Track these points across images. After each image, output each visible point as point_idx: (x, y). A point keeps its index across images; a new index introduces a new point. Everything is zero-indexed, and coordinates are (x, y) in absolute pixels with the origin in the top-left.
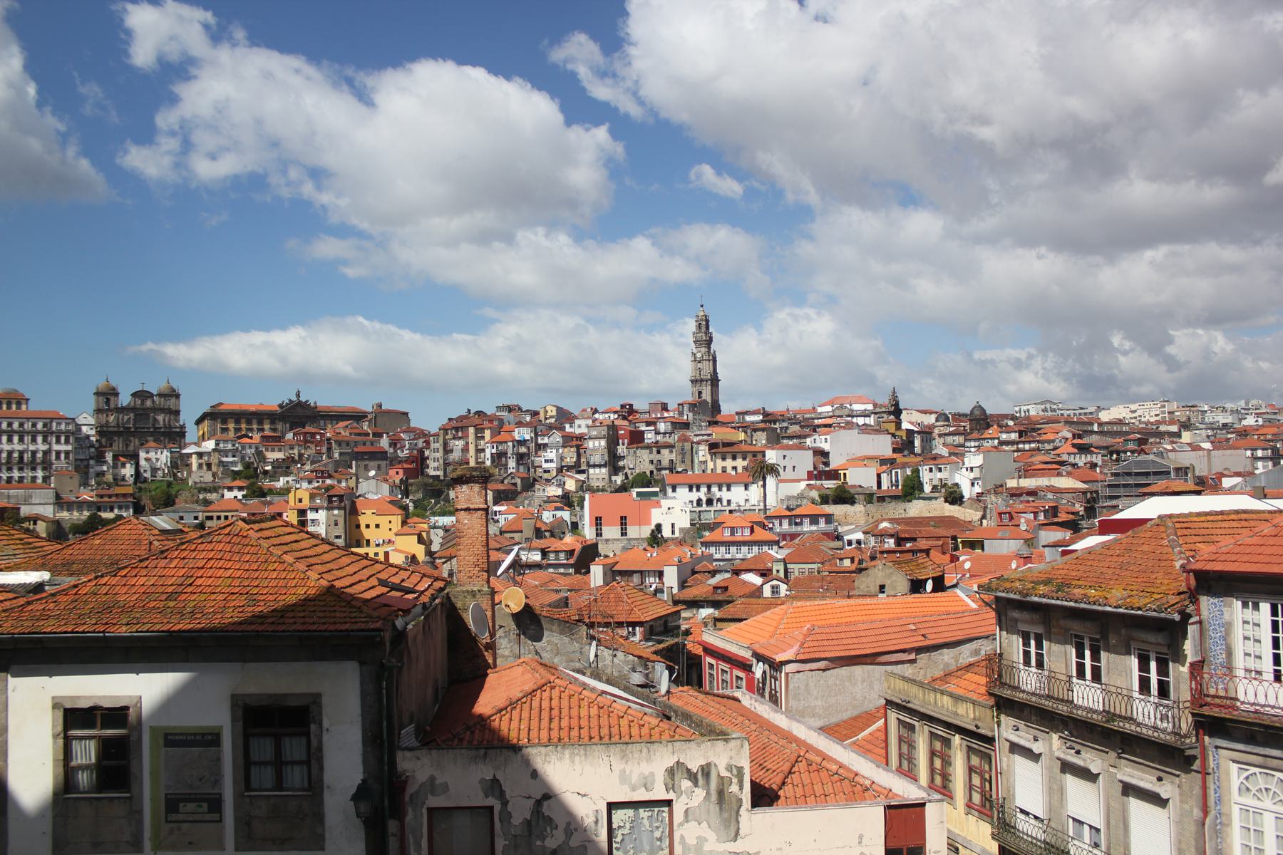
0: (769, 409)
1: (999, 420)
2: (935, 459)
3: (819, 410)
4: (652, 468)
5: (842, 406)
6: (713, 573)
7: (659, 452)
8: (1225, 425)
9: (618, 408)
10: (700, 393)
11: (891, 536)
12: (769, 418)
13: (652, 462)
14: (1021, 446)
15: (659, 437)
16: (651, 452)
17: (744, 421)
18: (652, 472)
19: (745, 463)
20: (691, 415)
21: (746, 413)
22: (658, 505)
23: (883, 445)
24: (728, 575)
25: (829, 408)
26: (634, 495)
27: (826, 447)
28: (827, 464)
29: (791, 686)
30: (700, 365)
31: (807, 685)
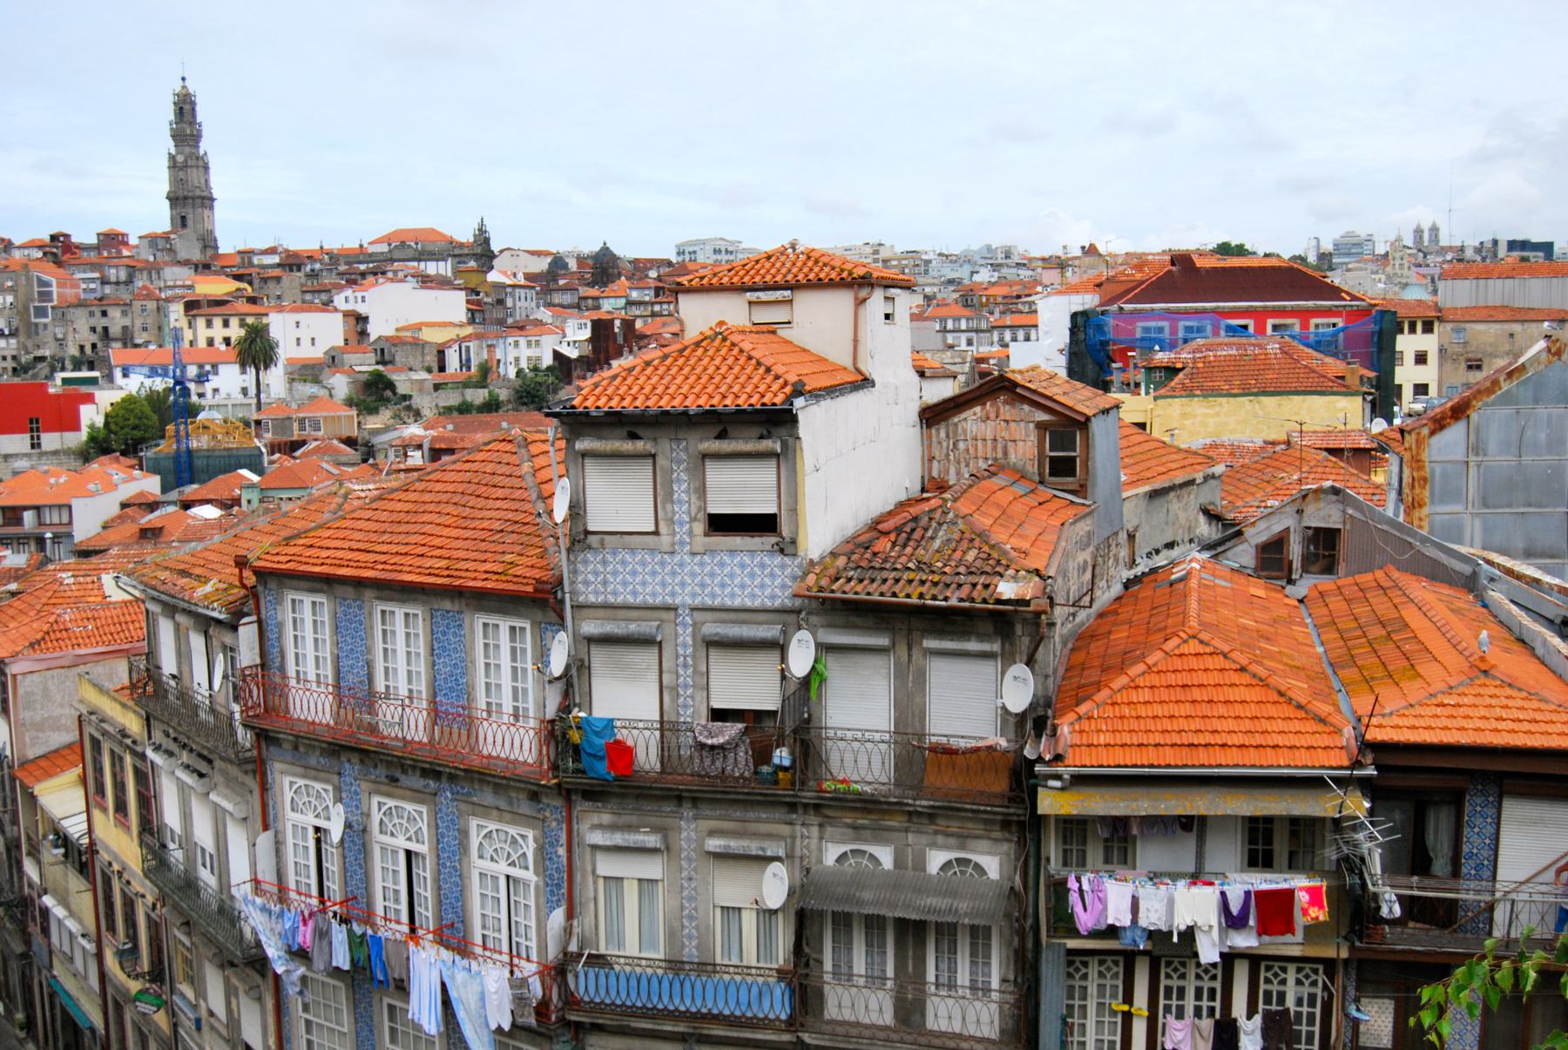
0: (294, 246)
1: (639, 267)
2: (522, 328)
3: (372, 249)
4: (94, 338)
5: (403, 243)
6: (153, 506)
7: (104, 314)
8: (951, 282)
9: (47, 239)
10: (183, 218)
11: (420, 447)
12: (292, 262)
13: (93, 330)
14: (657, 308)
15: (108, 290)
16: (92, 314)
17: (251, 264)
18: (94, 346)
19: (242, 332)
20: (159, 254)
21: (251, 252)
22: (90, 399)
23: (453, 306)
24: (171, 509)
25: (384, 248)
26: (59, 382)
27: (362, 309)
28: (363, 334)
29: (21, 691)
30: (181, 175)
31: (45, 689)
